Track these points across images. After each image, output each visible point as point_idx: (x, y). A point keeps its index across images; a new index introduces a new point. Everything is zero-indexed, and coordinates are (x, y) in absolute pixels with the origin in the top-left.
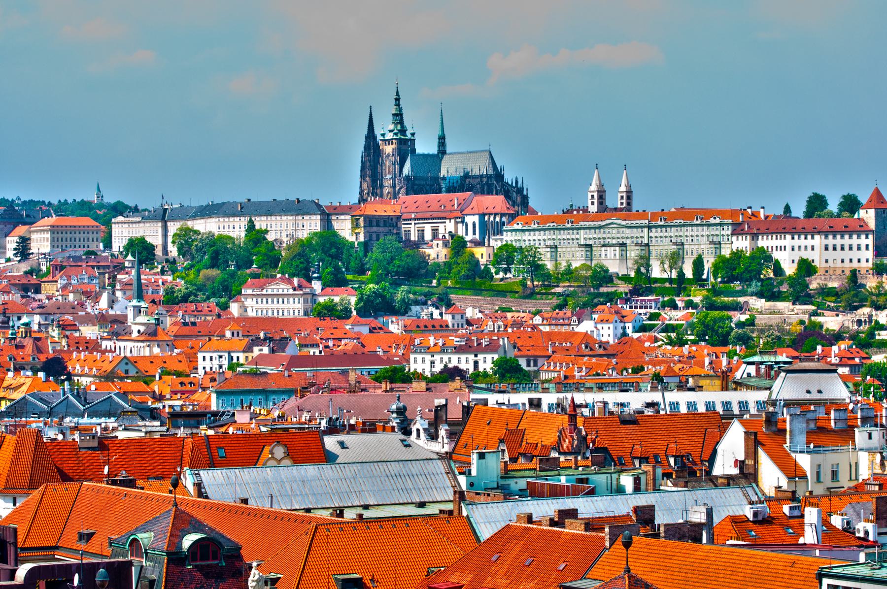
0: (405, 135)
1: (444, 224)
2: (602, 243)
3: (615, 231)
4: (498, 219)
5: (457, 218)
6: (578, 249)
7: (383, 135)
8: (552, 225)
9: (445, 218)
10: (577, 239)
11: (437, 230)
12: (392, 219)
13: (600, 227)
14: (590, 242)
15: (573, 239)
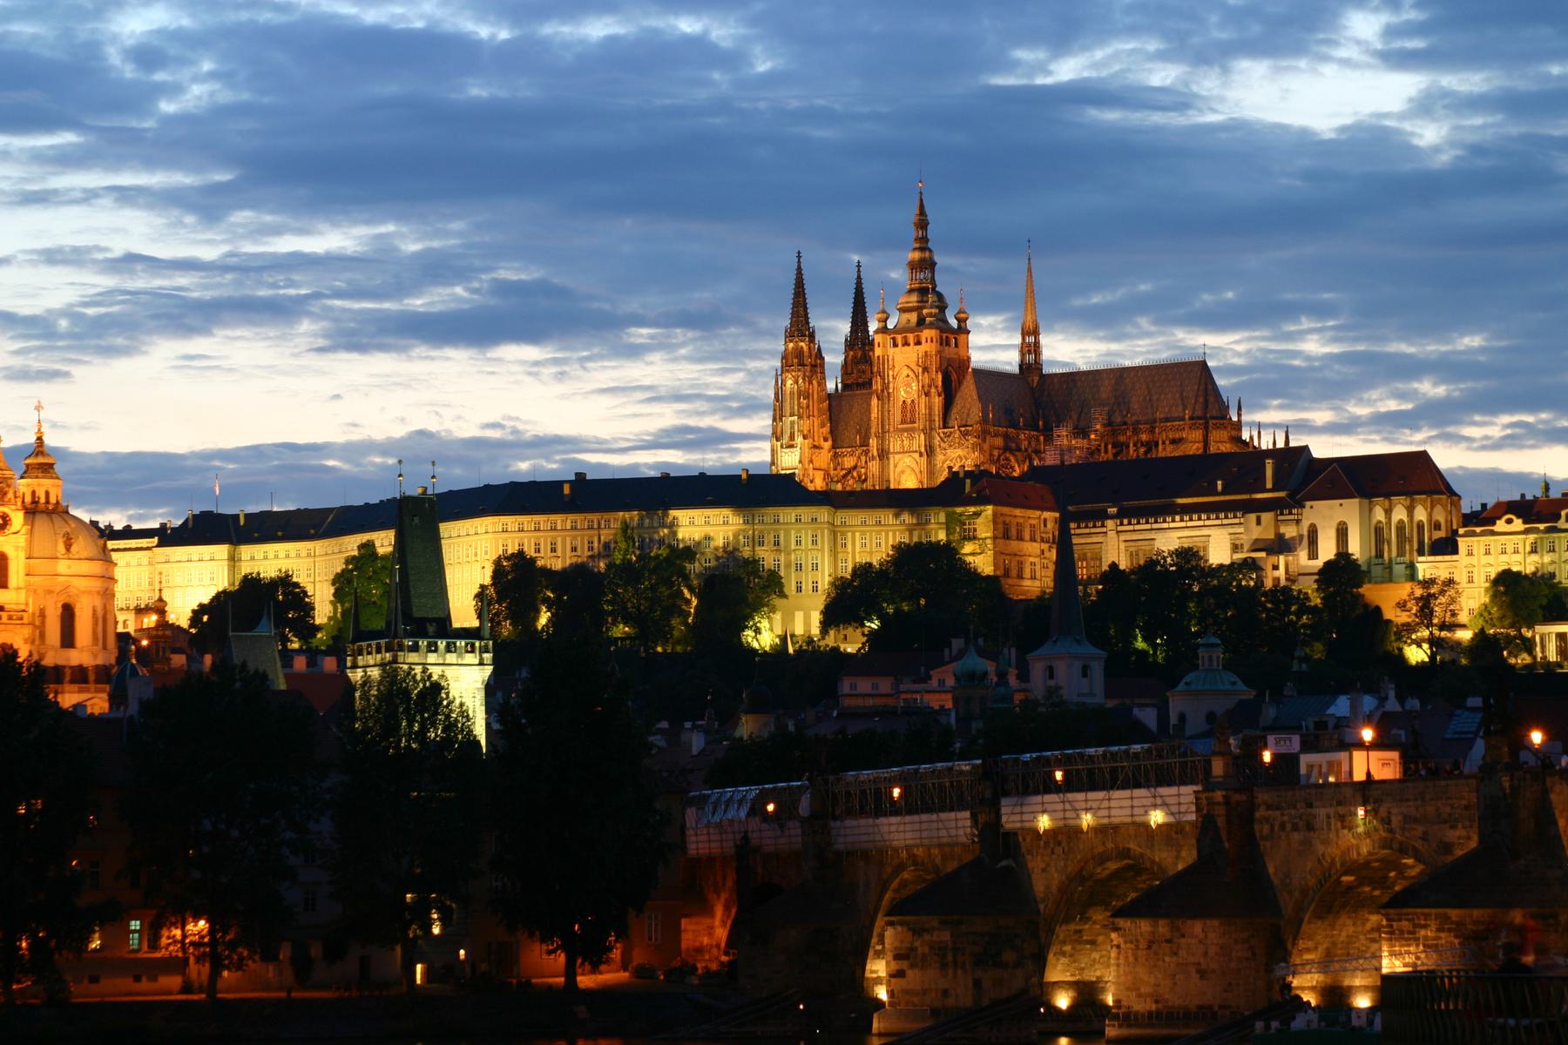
0: (946, 322)
4: (1421, 514)
11: (1205, 549)
12: (1045, 520)
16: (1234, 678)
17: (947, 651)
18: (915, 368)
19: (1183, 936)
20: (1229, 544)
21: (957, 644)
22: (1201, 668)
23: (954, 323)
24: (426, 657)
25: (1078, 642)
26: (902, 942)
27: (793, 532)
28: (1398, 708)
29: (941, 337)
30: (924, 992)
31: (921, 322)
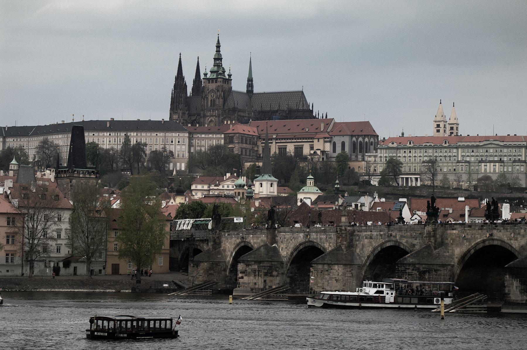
0: (225, 76)
1: (312, 143)
2: (479, 159)
3: (491, 150)
4: (366, 140)
5: (325, 138)
6: (458, 164)
7: (206, 75)
8: (428, 144)
9: (311, 138)
10: (455, 156)
11: (302, 148)
12: (254, 138)
13: (478, 147)
14: (468, 159)
15: (450, 156)
16: (317, 189)
17: (225, 177)
18: (214, 89)
19: (332, 269)
20: (309, 147)
21: (228, 175)
22: (307, 185)
23: (227, 77)
24: (80, 175)
25: (270, 176)
26: (243, 268)
27: (177, 139)
28: (379, 201)
29: (223, 81)
30: (249, 283)
31: (217, 75)
